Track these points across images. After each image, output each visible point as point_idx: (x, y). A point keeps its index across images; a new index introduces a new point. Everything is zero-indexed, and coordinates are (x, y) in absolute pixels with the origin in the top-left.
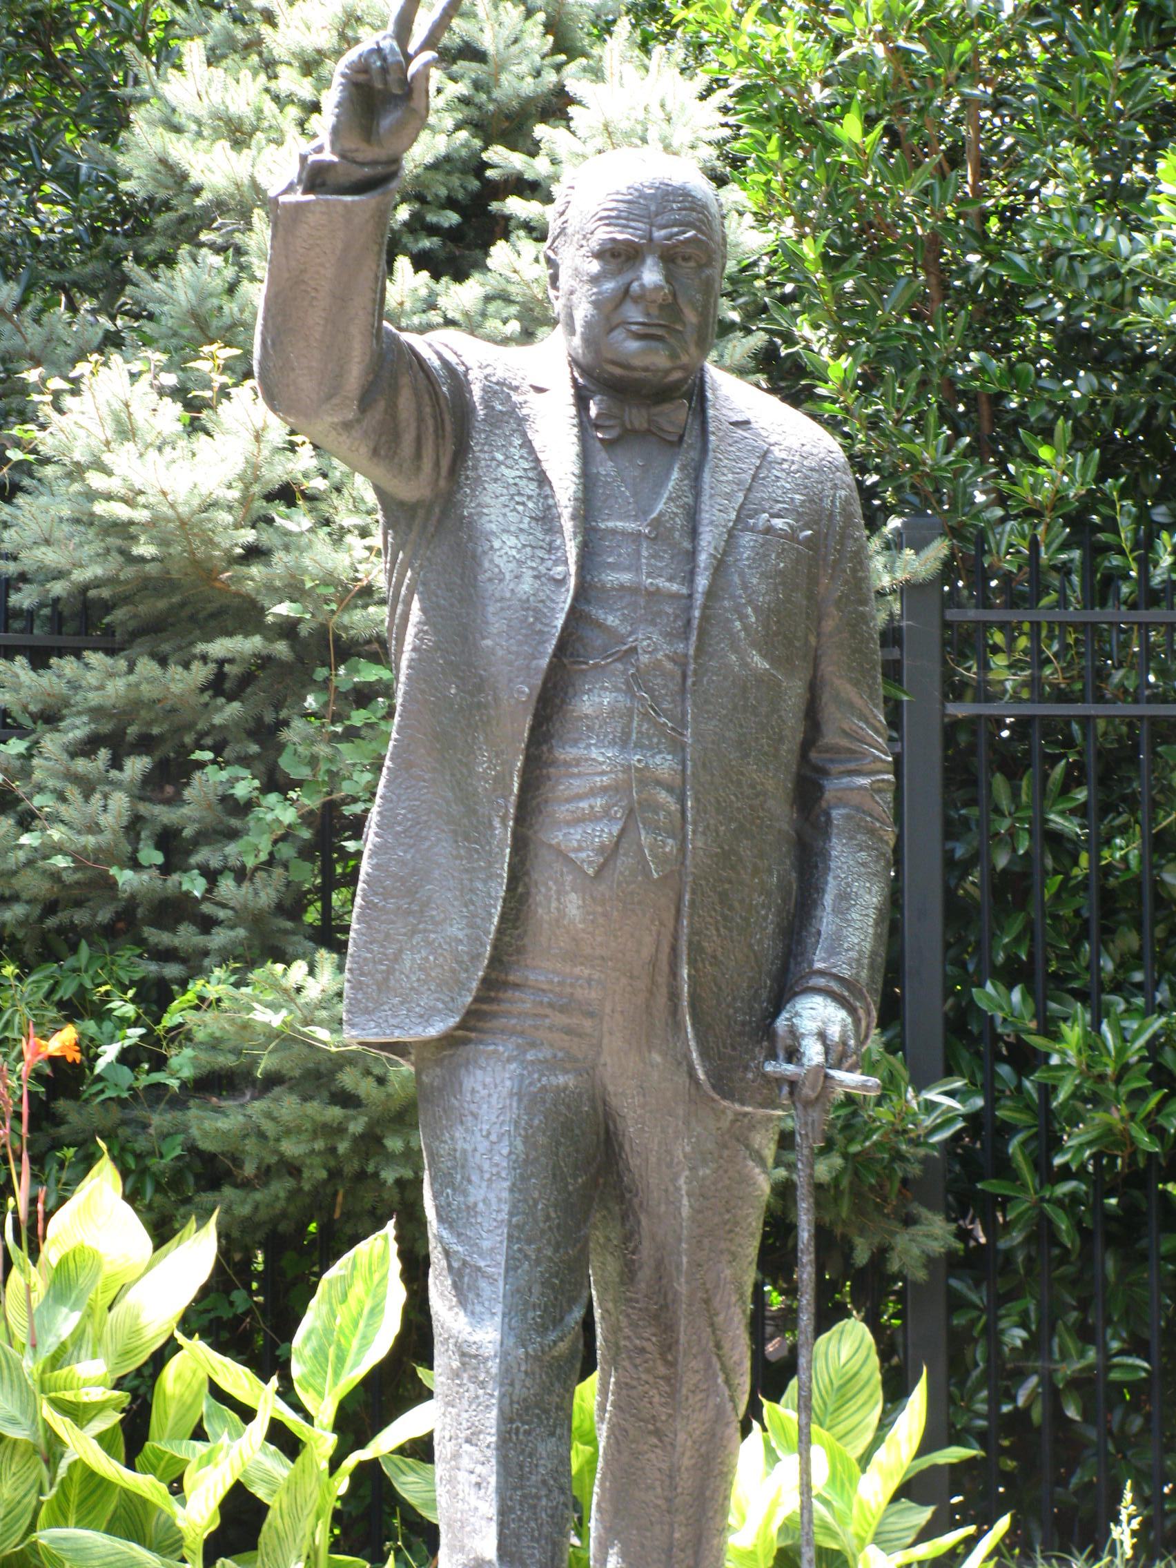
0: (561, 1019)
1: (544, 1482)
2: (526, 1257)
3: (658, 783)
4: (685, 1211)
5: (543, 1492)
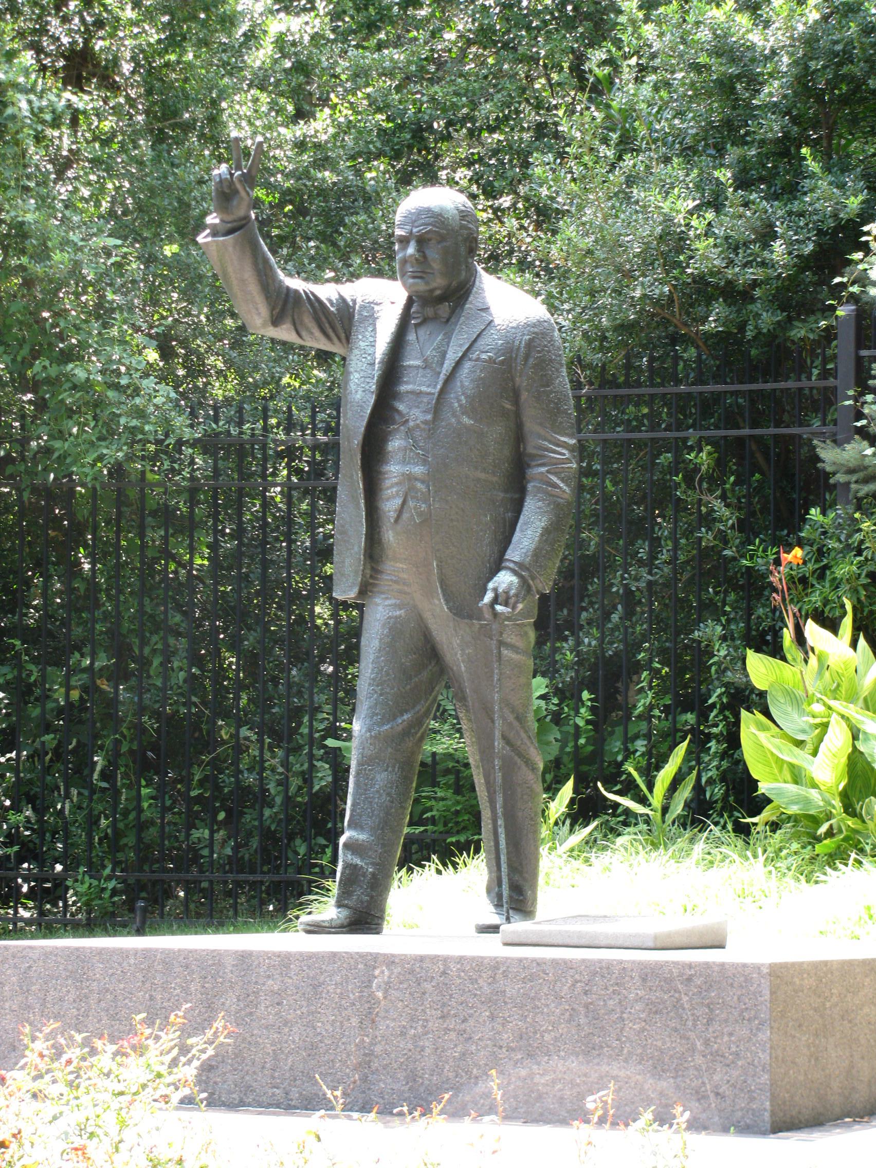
0: (396, 587)
1: (378, 792)
3: (416, 479)
4: (463, 669)
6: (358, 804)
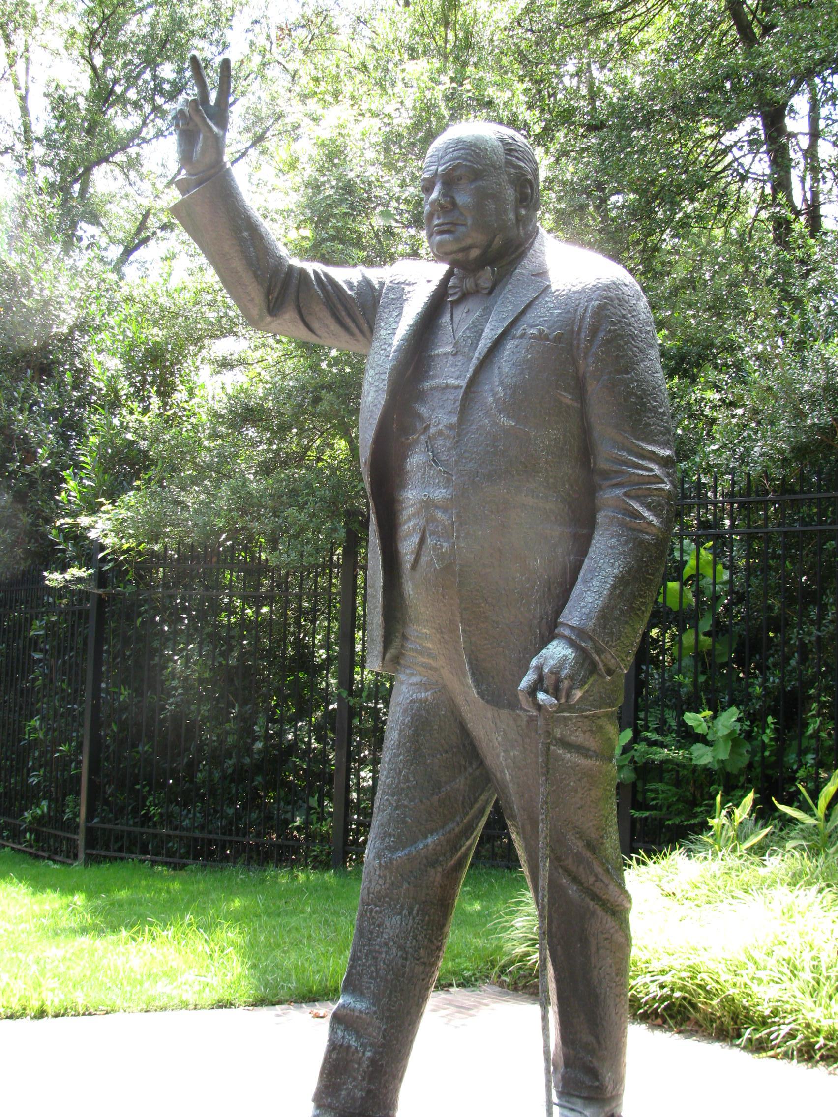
1: (386, 944)
2: (390, 804)
3: (437, 507)
4: (508, 777)
5: (384, 950)
6: (359, 958)
